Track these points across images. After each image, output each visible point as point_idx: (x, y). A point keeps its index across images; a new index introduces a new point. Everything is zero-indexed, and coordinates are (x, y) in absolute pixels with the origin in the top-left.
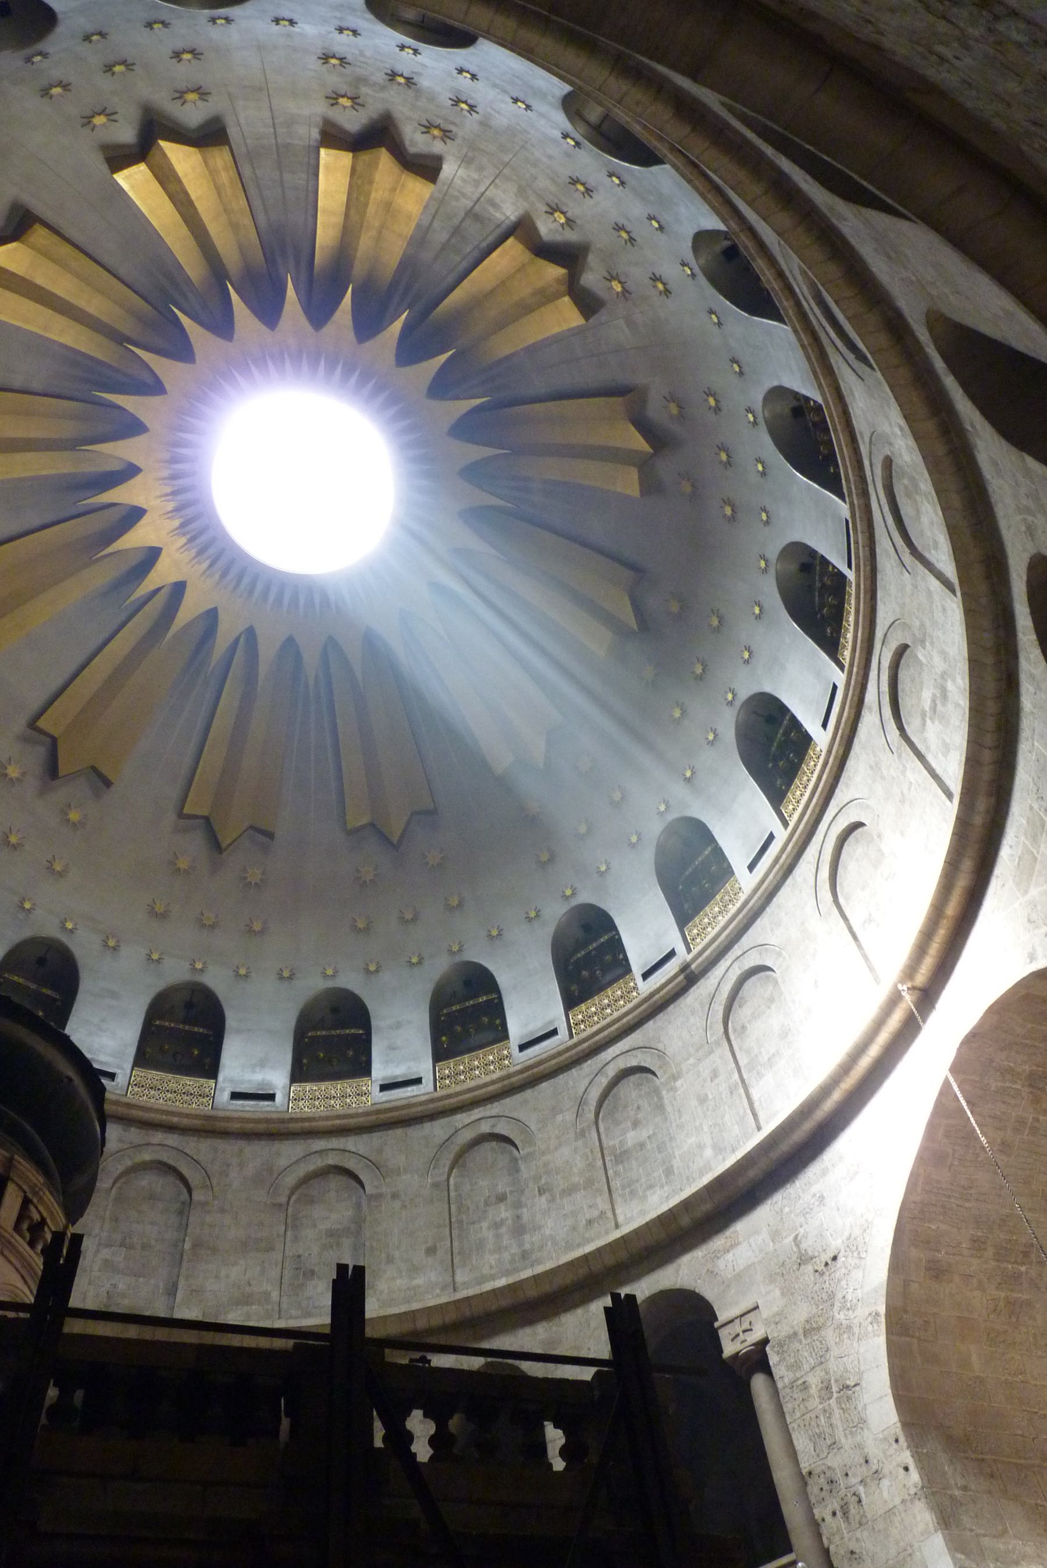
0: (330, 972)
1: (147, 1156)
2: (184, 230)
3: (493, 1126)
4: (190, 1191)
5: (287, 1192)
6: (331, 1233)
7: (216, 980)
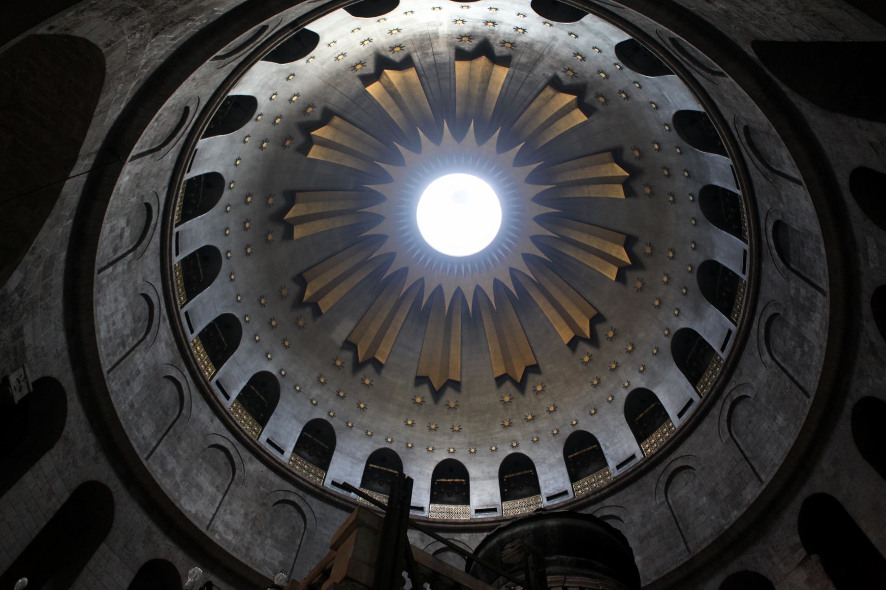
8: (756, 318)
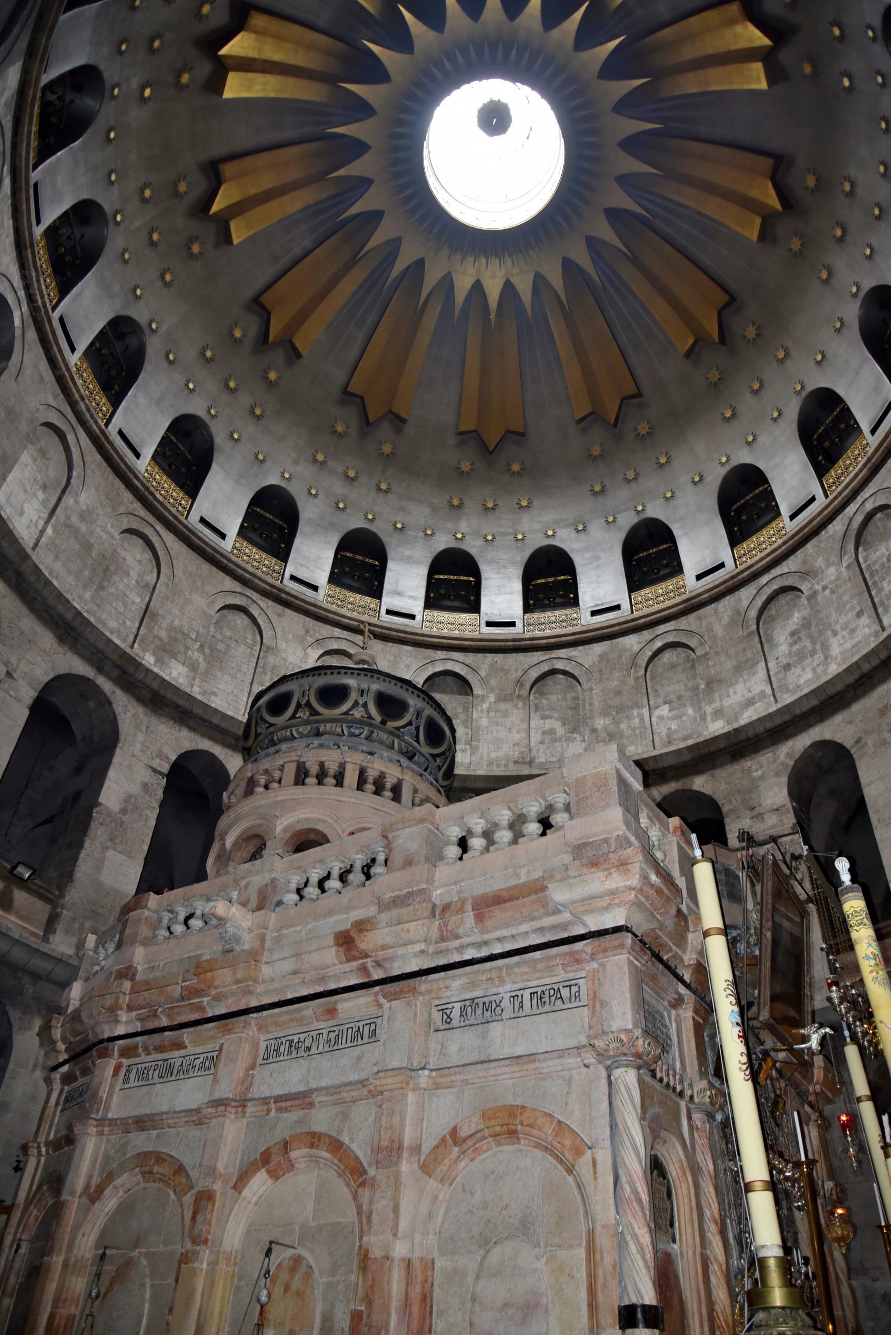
0: (724, 460)
1: (658, 644)
2: (291, 81)
3: (874, 503)
4: (693, 651)
5: (755, 622)
6: (793, 634)
7: (655, 510)
8: (345, 634)
